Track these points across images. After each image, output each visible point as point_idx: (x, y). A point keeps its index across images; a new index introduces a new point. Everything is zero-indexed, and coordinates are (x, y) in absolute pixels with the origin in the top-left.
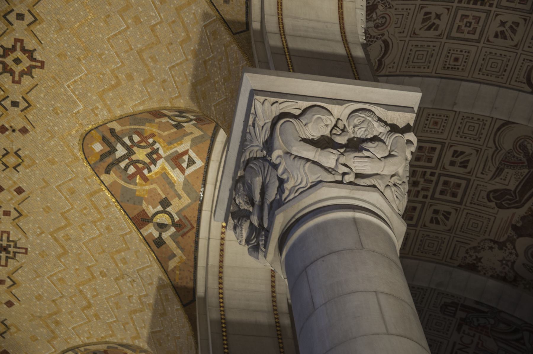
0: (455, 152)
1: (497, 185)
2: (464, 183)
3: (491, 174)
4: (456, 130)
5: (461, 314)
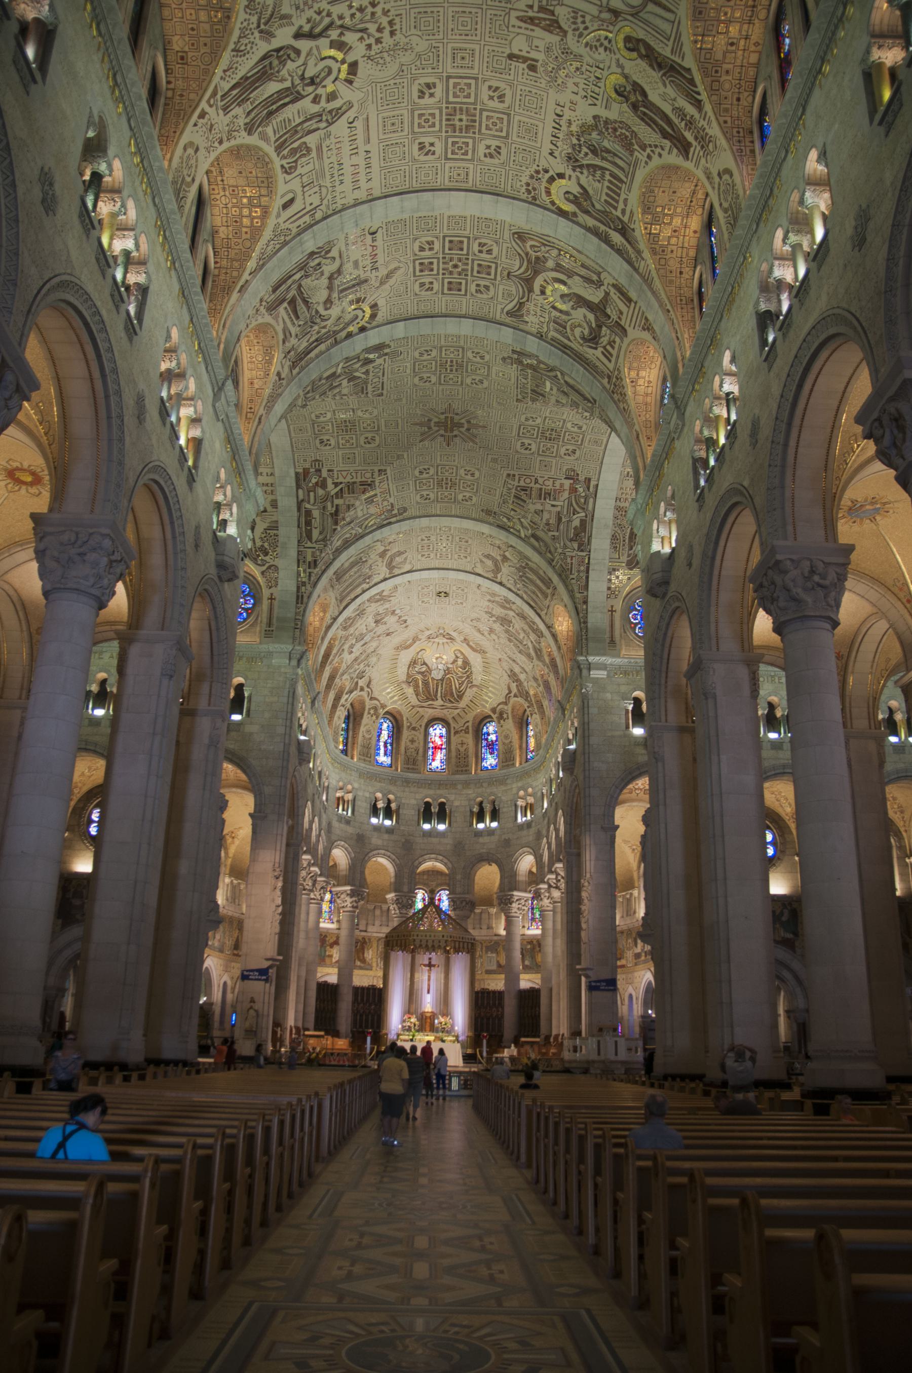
1: (404, 556)
5: (395, 512)
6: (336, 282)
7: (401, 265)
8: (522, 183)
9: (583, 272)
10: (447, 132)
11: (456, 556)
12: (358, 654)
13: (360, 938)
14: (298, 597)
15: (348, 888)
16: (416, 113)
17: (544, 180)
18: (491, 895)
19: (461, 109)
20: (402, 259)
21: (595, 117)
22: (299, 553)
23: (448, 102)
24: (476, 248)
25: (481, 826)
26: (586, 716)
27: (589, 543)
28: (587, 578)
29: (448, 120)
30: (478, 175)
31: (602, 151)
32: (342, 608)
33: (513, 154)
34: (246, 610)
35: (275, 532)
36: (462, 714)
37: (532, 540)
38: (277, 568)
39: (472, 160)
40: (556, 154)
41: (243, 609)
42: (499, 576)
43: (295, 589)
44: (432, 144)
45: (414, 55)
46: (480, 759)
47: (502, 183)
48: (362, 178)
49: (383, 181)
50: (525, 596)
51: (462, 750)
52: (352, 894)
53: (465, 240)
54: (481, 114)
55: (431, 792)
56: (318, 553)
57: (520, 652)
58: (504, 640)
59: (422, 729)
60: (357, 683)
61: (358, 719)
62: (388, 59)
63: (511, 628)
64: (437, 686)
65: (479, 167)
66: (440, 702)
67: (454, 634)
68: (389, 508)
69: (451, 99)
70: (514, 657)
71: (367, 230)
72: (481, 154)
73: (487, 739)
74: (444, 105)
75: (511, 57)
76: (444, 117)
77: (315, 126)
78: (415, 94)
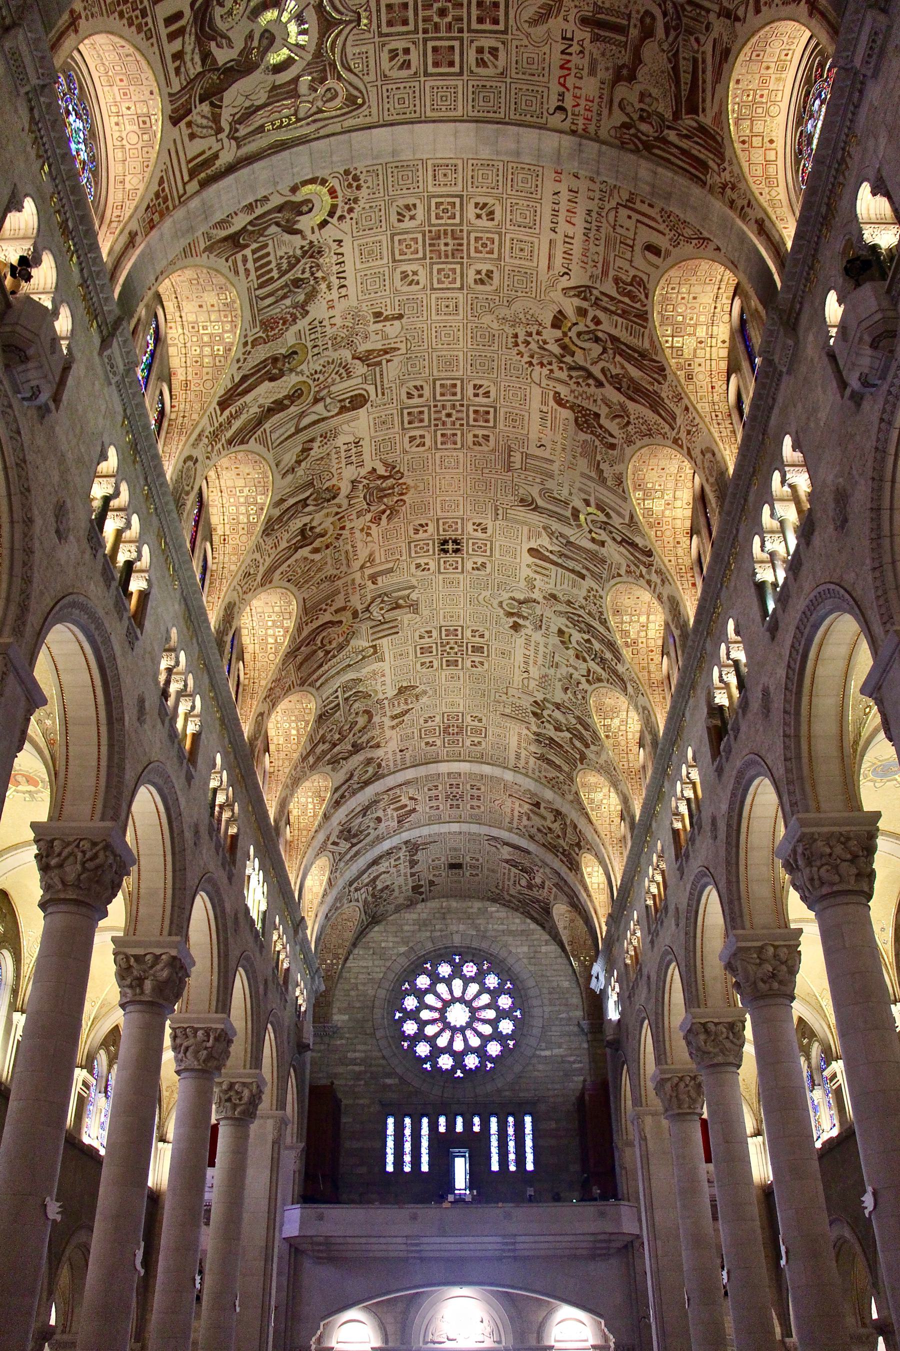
6: (625, 58)
7: (526, 25)
8: (365, 186)
9: (258, 120)
10: (461, 231)
16: (495, 256)
17: (341, 204)
19: (447, 256)
20: (526, 42)
21: (307, 312)
23: (462, 264)
24: (414, 56)
29: (461, 245)
30: (420, 179)
31: (290, 291)
33: (383, 218)
39: (430, 197)
40: (334, 246)
44: (479, 216)
45: (496, 313)
47: (390, 175)
48: (564, 205)
49: (539, 183)
53: (431, 69)
54: (425, 254)
62: (521, 316)
65: (421, 189)
69: (458, 267)
71: (569, 120)
72: (420, 207)
74: (465, 260)
75: (400, 317)
76: (465, 248)
77: (605, 299)
78: (496, 275)
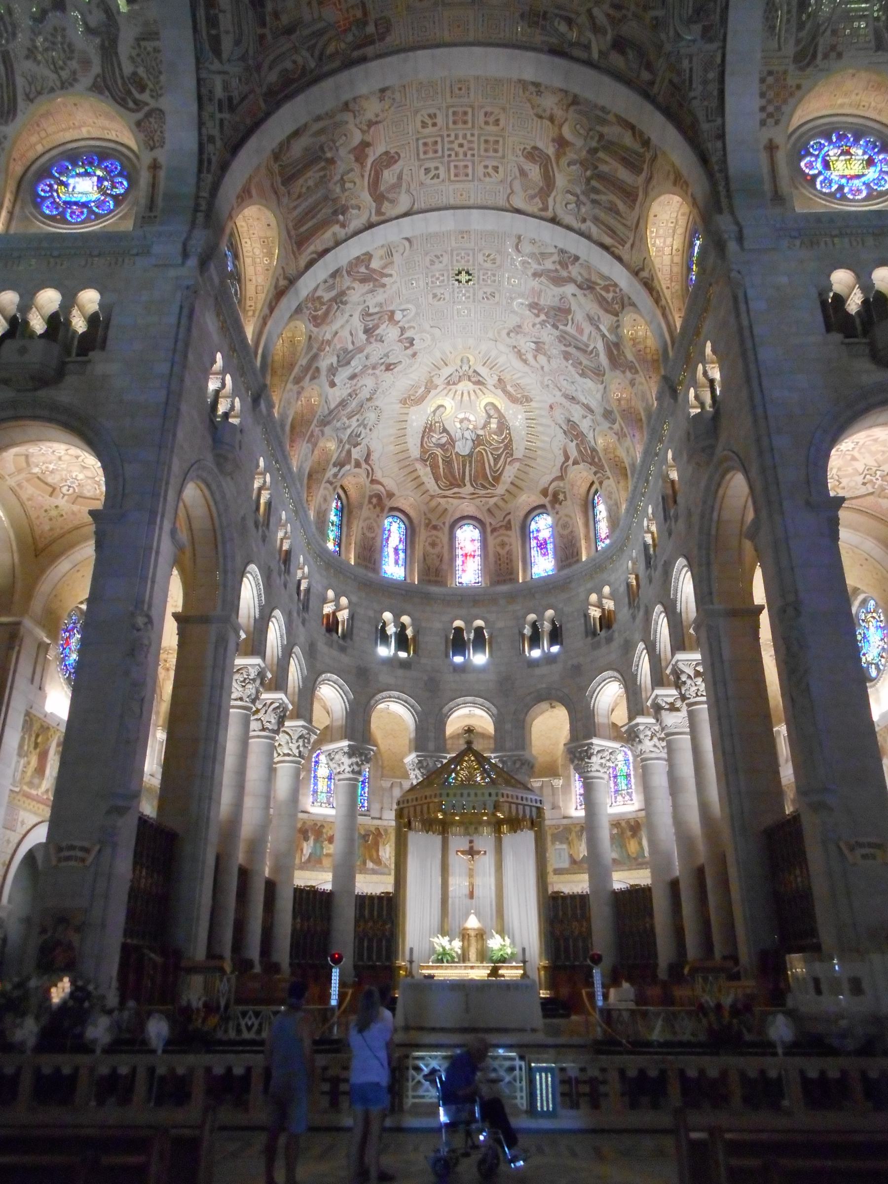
0: (438, 178)
1: (397, 168)
2: (422, 156)
3: (405, 172)
4: (444, 193)
5: (371, 29)
11: (480, 170)
12: (345, 393)
13: (373, 829)
14: (201, 162)
15: (345, 743)
18: (555, 761)
22: (199, 81)
25: (536, 653)
26: (744, 316)
27: (724, 21)
28: (722, 92)
32: (302, 263)
34: (115, 198)
35: (156, 44)
36: (501, 503)
37: (616, 60)
38: (160, 113)
41: (110, 195)
42: (551, 201)
43: (195, 147)
46: (527, 563)
50: (595, 231)
51: (503, 552)
52: (352, 752)
55: (463, 612)
56: (235, 83)
57: (583, 375)
58: (558, 362)
59: (446, 529)
60: (349, 452)
61: (355, 511)
63: (569, 328)
64: (464, 466)
66: (468, 489)
67: (483, 371)
68: (359, 14)
70: (571, 390)
73: (536, 538)
